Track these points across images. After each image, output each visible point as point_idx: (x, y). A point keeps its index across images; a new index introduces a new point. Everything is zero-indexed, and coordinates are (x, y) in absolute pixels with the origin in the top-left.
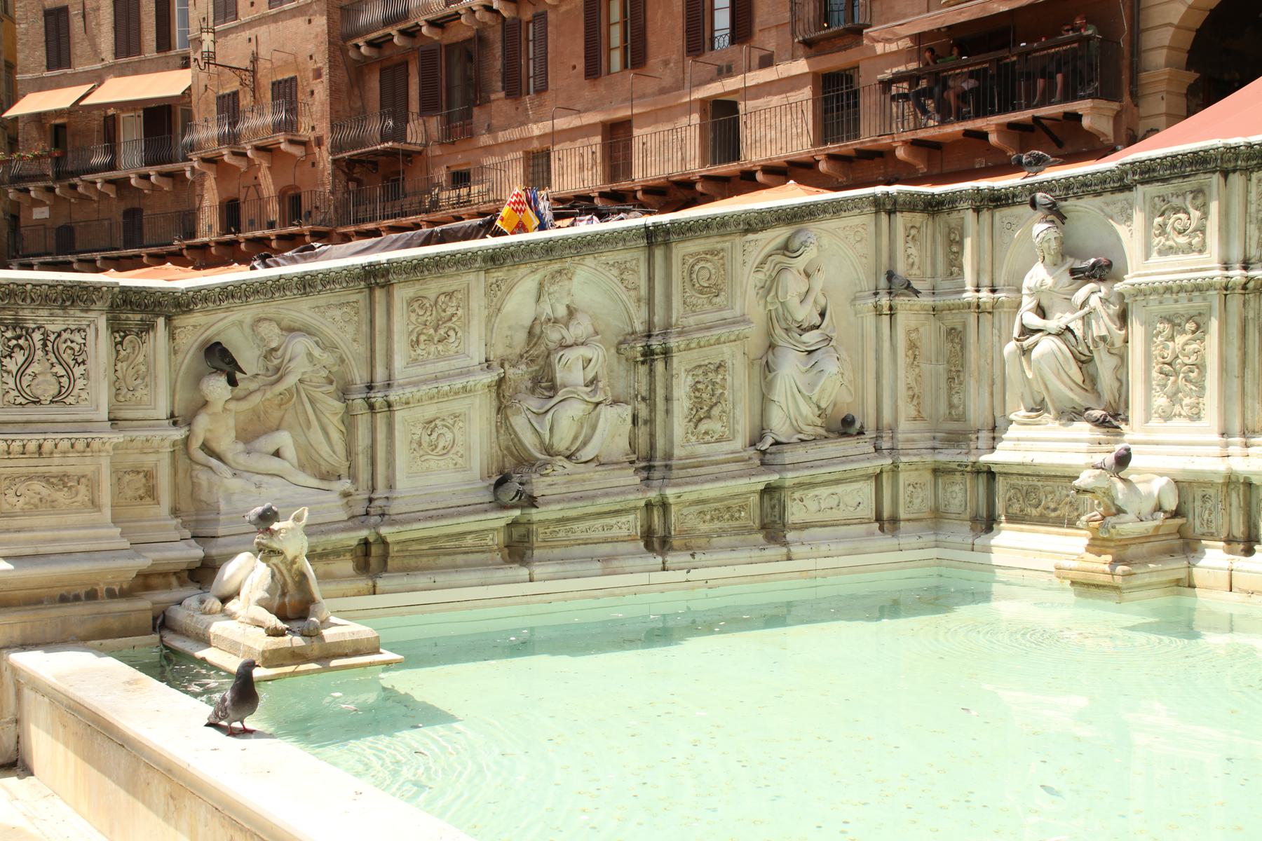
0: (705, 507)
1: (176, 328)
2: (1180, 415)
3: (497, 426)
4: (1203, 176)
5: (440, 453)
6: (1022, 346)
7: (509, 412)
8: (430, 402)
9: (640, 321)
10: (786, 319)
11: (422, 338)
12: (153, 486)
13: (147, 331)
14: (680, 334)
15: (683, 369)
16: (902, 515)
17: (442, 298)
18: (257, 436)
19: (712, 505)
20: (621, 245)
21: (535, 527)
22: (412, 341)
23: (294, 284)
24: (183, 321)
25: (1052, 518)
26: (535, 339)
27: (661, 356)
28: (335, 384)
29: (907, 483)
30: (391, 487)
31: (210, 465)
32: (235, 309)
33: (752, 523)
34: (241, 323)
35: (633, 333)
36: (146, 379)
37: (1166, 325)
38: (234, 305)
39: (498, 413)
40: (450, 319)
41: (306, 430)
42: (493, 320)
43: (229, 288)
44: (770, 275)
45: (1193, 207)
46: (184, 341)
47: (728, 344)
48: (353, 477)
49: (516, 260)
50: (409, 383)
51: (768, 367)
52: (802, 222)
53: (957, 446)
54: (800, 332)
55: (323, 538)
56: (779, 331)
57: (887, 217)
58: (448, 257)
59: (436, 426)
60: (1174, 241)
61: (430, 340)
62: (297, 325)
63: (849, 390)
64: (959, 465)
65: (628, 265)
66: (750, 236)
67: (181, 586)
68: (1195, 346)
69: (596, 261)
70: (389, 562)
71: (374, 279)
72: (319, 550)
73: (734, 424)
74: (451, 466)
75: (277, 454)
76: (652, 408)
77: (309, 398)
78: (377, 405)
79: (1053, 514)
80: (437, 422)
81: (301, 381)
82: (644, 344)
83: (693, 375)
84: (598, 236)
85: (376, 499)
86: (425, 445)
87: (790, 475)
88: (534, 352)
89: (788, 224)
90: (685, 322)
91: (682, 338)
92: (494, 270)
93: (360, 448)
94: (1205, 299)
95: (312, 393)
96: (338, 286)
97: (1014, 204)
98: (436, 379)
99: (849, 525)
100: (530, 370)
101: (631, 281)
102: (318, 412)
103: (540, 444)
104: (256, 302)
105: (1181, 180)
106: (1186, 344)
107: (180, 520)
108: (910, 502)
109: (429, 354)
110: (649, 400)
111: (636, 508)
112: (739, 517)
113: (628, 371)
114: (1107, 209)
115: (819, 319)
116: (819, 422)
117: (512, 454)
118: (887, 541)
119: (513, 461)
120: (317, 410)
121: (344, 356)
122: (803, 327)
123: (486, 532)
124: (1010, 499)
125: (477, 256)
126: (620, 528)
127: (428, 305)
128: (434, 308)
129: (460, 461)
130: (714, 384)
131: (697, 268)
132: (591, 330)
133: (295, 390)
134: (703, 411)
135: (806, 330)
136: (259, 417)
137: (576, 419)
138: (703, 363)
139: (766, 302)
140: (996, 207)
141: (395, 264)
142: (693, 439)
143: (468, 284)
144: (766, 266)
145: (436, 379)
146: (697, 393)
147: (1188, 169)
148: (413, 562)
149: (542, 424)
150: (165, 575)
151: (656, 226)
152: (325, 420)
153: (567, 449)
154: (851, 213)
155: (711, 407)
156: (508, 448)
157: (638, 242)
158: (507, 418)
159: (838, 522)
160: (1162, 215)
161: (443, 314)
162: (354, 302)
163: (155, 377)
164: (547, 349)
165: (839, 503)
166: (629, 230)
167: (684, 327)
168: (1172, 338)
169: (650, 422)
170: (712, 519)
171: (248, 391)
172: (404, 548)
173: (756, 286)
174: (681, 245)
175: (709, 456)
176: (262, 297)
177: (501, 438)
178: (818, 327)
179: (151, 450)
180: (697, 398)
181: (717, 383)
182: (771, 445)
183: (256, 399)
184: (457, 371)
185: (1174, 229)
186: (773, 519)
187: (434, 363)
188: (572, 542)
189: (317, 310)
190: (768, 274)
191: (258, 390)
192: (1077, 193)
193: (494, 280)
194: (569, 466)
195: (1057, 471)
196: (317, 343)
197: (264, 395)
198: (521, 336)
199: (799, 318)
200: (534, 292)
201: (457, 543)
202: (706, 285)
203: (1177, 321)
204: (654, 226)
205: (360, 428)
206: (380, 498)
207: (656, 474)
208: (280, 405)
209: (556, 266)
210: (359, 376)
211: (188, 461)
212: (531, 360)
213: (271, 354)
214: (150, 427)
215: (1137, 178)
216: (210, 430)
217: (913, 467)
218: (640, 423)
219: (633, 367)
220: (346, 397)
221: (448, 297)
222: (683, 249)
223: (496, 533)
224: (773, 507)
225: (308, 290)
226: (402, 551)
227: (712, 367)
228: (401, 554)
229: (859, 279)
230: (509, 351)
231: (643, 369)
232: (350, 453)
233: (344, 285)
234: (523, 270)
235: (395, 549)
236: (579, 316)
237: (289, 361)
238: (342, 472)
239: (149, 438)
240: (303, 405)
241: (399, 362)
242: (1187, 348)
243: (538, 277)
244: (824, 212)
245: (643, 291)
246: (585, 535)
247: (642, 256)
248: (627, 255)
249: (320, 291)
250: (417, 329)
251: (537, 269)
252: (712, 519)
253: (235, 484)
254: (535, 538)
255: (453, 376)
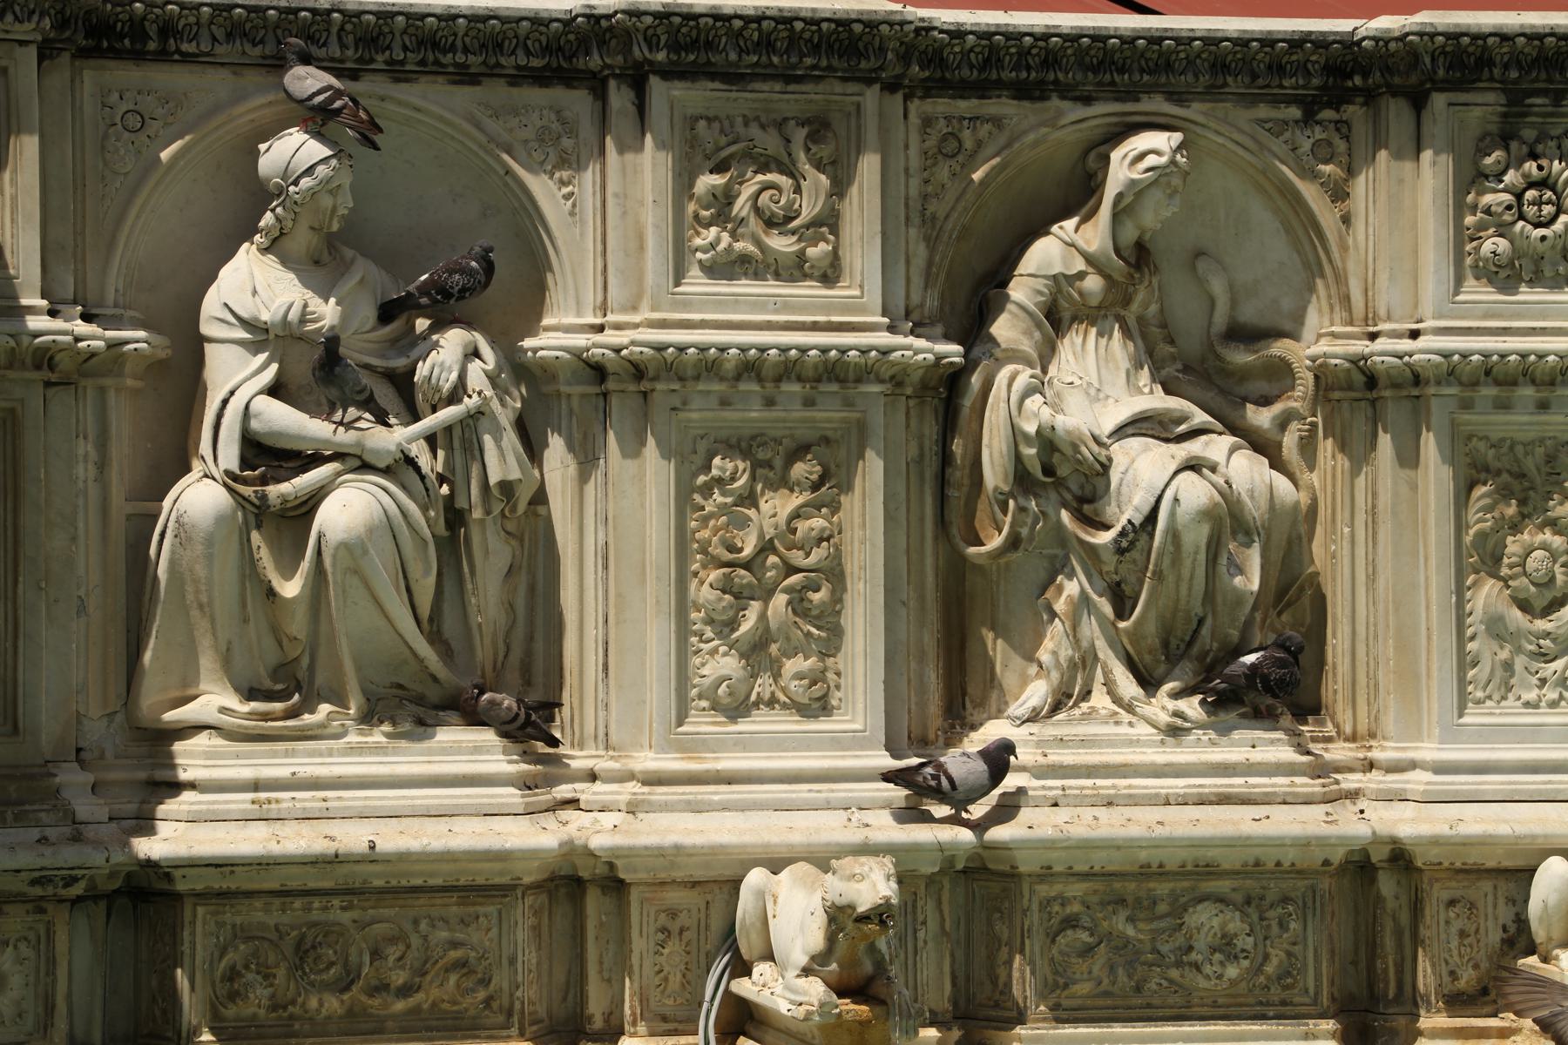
2: (772, 702)
4: (838, 87)
6: (264, 497)
25: (394, 1017)
37: (741, 465)
45: (810, 161)
53: (17, 818)
60: (758, 243)
64: (34, 882)
68: (817, 523)
79: (400, 1006)
94: (848, 403)
97: (163, 56)
105: (778, 87)
106: (796, 515)
114: (492, 125)
124: (232, 974)
140: (83, 53)
147: (809, 61)
160: (718, 169)
168: (749, 499)
185: (757, 210)
192: (402, 63)
195: (432, 875)
203: (762, 455)
215: (661, 56)
242: (802, 526)
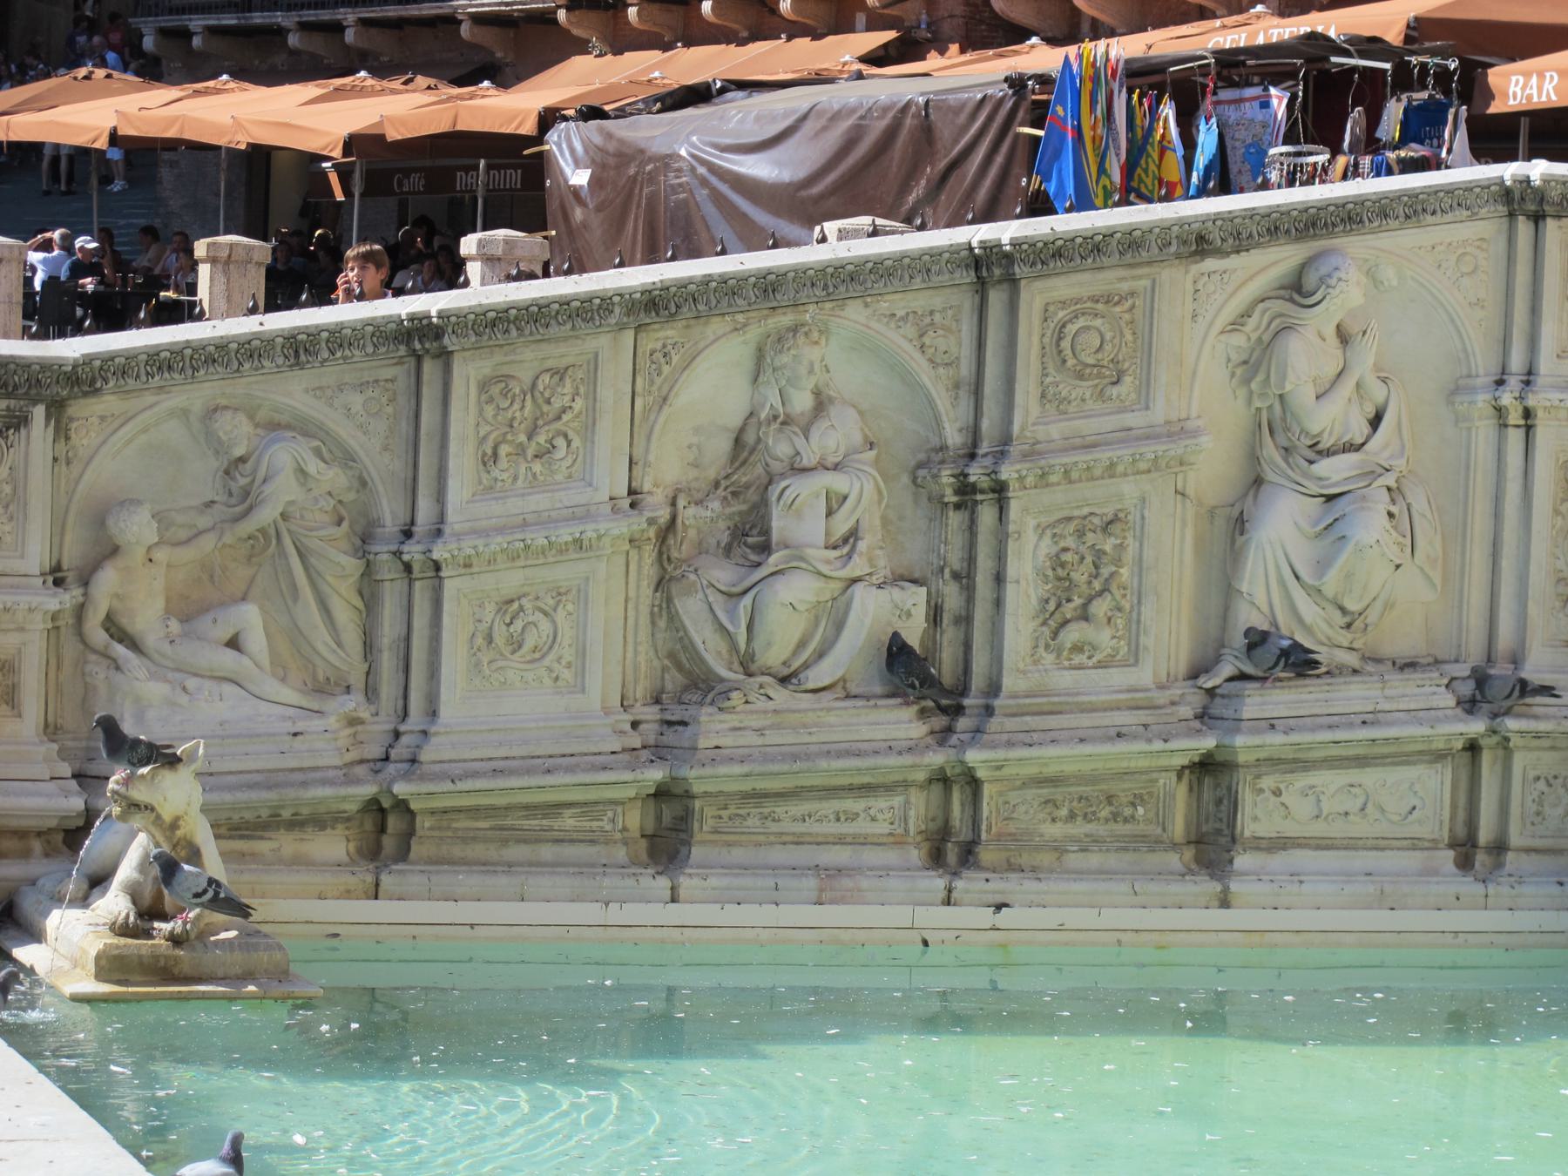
0: (1058, 793)
1: (71, 419)
3: (652, 614)
5: (528, 658)
7: (675, 589)
8: (509, 565)
9: (958, 425)
10: (1287, 429)
11: (504, 450)
12: (13, 685)
13: (17, 428)
14: (1025, 456)
15: (1032, 523)
16: (1515, 839)
17: (546, 378)
18: (205, 609)
19: (1072, 789)
20: (919, 279)
21: (697, 804)
22: (484, 454)
23: (279, 349)
24: (79, 408)
26: (745, 454)
27: (991, 496)
28: (345, 524)
29: (1532, 774)
30: (433, 714)
31: (114, 655)
32: (174, 389)
33: (1159, 831)
34: (185, 413)
35: (941, 449)
36: (11, 508)
38: (172, 382)
39: (656, 590)
40: (559, 418)
41: (290, 603)
42: (652, 417)
43: (163, 355)
44: (1260, 339)
46: (85, 442)
47: (1131, 478)
48: (371, 692)
49: (701, 307)
50: (475, 532)
51: (1240, 524)
52: (1331, 235)
54: (1311, 455)
55: (291, 793)
56: (1270, 451)
57: (1531, 225)
58: (556, 306)
59: (521, 609)
61: (521, 451)
62: (284, 418)
63: (1428, 578)
65: (937, 317)
66: (1210, 264)
67: (47, 855)
69: (869, 311)
70: (414, 847)
71: (420, 341)
72: (286, 814)
73: (1138, 635)
74: (547, 681)
75: (234, 643)
76: (969, 591)
77: (296, 547)
78: (416, 567)
80: (524, 601)
81: (284, 516)
82: (956, 471)
83: (1054, 535)
84: (870, 265)
85: (404, 733)
86: (499, 640)
87: (1239, 741)
88: (743, 477)
89: (1297, 240)
90: (1041, 432)
91: (1027, 465)
92: (656, 326)
93: (386, 641)
95: (303, 540)
96: (357, 352)
98: (525, 524)
99: (1383, 849)
100: (728, 510)
101: (943, 348)
102: (314, 575)
103: (730, 651)
104: (211, 377)
107: (55, 746)
108: (1538, 814)
109: (515, 478)
110: (965, 578)
111: (906, 785)
112: (1133, 817)
113: (931, 520)
115: (1366, 429)
116: (1344, 638)
117: (679, 667)
118: (1468, 886)
119: (680, 679)
120: (312, 570)
121: (365, 475)
122: (1320, 447)
123: (601, 807)
125: (613, 304)
126: (873, 819)
127: (517, 391)
128: (529, 397)
129: (567, 675)
130: (1099, 553)
131: (1072, 329)
132: (857, 438)
133: (272, 532)
134: (1071, 605)
135: (1328, 453)
136: (212, 577)
137: (801, 607)
138: (1076, 513)
139: (1251, 393)
141: (453, 319)
142: (1049, 658)
143: (596, 355)
144: (1252, 323)
145: (525, 524)
146: (1060, 571)
148: (457, 851)
149: (732, 613)
150: (21, 834)
151: (991, 248)
152: (325, 589)
153: (784, 663)
154: (1449, 217)
155: (1090, 600)
156: (672, 656)
157: (957, 275)
158: (669, 600)
159: (1361, 843)
161: (545, 408)
162: (386, 380)
163: (26, 504)
164: (768, 473)
165: (1365, 804)
166: (935, 254)
167: (1038, 442)
169: (965, 620)
170: (1072, 816)
171: (194, 531)
172: (445, 824)
173: (1229, 360)
174: (1039, 284)
175: (1078, 694)
176: (219, 369)
177: (659, 636)
178: (1358, 448)
179: (12, 626)
180: (1059, 579)
181: (1105, 553)
182: (1231, 679)
183: (208, 543)
184: (565, 512)
186: (1218, 825)
187: (523, 495)
188: (772, 838)
189: (318, 392)
190: (1254, 336)
191: (213, 528)
193: (659, 345)
194: (781, 695)
196: (318, 453)
197: (220, 539)
198: (721, 446)
199: (1315, 428)
200: (748, 364)
201: (544, 822)
202: (1091, 361)
204: (985, 248)
205: (387, 605)
206: (412, 732)
207: (963, 723)
208: (249, 558)
209: (786, 319)
210: (390, 514)
211: (81, 647)
212: (734, 494)
213: (237, 467)
214: (12, 587)
216: (117, 596)
217: (1546, 743)
218: (945, 621)
219: (939, 512)
220: (367, 548)
221: (557, 378)
222: (1037, 295)
223: (619, 809)
224: (1219, 802)
225: (303, 358)
226: (440, 828)
227: (1096, 521)
228: (436, 833)
229: (1465, 350)
230: (693, 473)
231: (955, 519)
232: (369, 647)
233: (370, 349)
234: (717, 326)
235: (427, 824)
236: (833, 411)
237: (264, 481)
238: (352, 681)
239: (8, 606)
240: (286, 558)
241: (458, 492)
243: (754, 333)
244: (1384, 214)
245: (966, 369)
246: (800, 828)
247: (966, 302)
248: (937, 300)
249: (325, 360)
250: (493, 436)
251: (745, 325)
252: (1072, 816)
253: (155, 690)
254: (696, 825)
255: (557, 521)
